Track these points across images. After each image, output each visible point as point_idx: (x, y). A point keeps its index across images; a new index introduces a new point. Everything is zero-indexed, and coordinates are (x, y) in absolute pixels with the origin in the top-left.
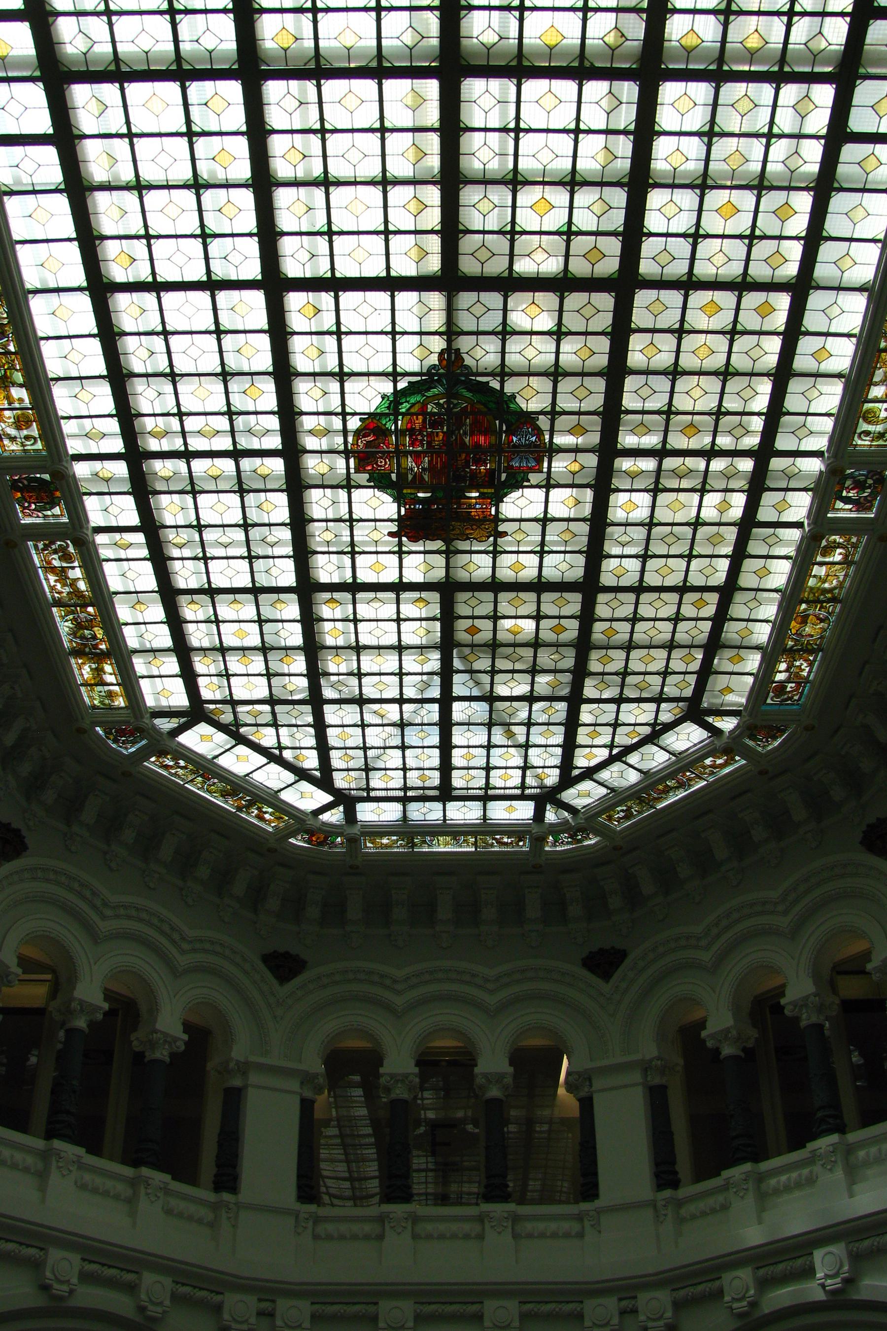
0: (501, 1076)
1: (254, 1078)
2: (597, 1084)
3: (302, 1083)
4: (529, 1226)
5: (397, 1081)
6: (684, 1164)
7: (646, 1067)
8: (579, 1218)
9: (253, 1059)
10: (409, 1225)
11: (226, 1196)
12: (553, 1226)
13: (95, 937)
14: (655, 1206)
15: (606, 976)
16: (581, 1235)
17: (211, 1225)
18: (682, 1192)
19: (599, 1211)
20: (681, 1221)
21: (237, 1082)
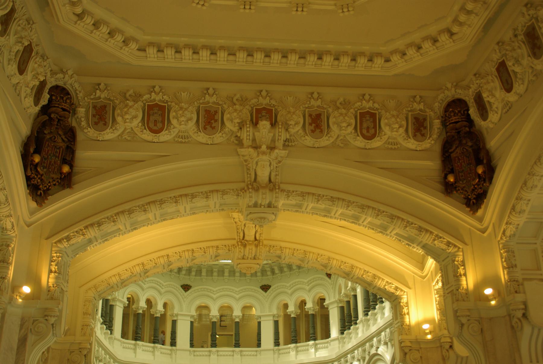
0: (239, 316)
1: (179, 317)
2: (262, 319)
3: (191, 317)
4: (244, 353)
5: (214, 317)
6: (281, 340)
7: (274, 316)
8: (256, 351)
9: (179, 313)
10: (216, 353)
11: (174, 348)
12: (250, 353)
13: (143, 289)
14: (274, 350)
15: (266, 291)
16: (256, 355)
17: (170, 354)
18: (280, 347)
19: (261, 351)
20: (280, 354)
21: (175, 319)
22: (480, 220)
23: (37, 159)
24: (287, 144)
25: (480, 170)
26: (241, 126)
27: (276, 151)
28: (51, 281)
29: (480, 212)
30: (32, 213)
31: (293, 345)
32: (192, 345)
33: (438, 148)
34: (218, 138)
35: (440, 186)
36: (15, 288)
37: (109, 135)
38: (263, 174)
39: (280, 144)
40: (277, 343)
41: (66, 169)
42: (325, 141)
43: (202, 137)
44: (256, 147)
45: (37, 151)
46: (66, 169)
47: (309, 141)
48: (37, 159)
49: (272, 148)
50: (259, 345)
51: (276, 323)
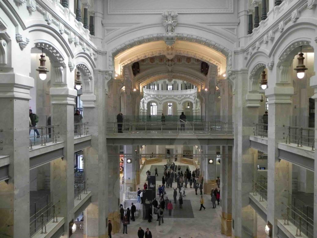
7: (181, 83)
22: (207, 77)
23: (134, 69)
24: (174, 64)
25: (207, 69)
26: (166, 61)
27: (172, 66)
28: (138, 88)
29: (207, 76)
30: (134, 77)
31: (185, 90)
32: (162, 90)
33: (201, 63)
34: (162, 63)
35: (200, 71)
36: (133, 89)
37: (145, 63)
38: (170, 70)
39: (173, 64)
40: (182, 89)
41: (138, 70)
42: (181, 63)
43: (160, 63)
44: (169, 65)
45: (134, 68)
46: (138, 70)
47: (178, 63)
48: (134, 69)
49: (171, 65)
50: (178, 90)
51: (182, 85)
